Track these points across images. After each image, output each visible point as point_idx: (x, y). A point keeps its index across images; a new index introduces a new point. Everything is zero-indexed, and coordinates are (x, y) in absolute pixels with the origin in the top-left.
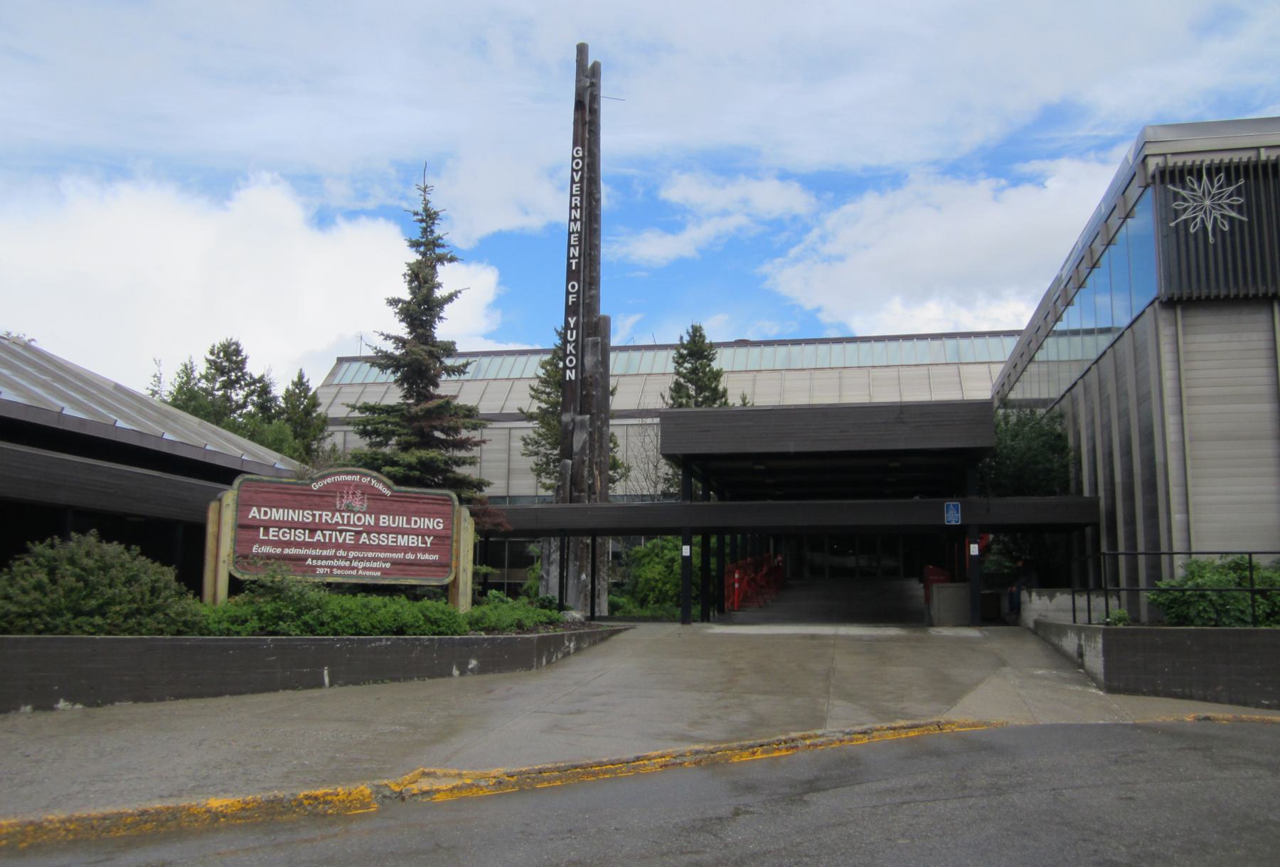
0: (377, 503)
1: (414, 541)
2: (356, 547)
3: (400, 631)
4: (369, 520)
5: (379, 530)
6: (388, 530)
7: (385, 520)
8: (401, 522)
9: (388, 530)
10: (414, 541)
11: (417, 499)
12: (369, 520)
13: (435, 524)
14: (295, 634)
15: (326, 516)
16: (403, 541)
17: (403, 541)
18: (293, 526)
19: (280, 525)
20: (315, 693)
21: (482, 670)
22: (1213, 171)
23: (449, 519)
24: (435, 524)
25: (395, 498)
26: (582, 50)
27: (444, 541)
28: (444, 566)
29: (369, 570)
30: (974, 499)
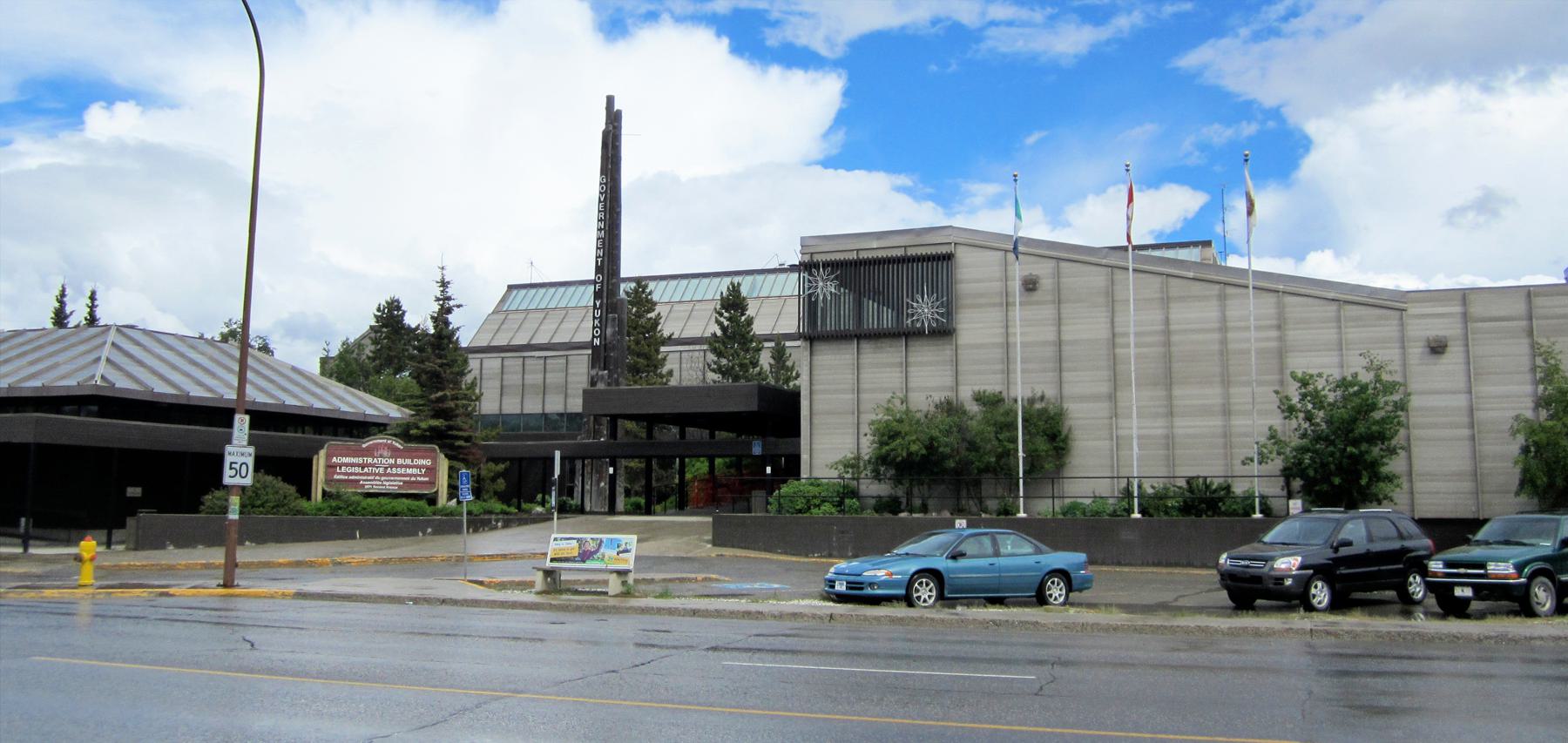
0: (396, 453)
1: (415, 471)
2: (385, 475)
3: (395, 515)
4: (392, 461)
5: (397, 466)
6: (401, 466)
7: (400, 461)
8: (408, 462)
9: (401, 466)
10: (415, 471)
11: (417, 450)
12: (392, 461)
13: (427, 462)
14: (345, 516)
15: (370, 460)
16: (409, 471)
17: (409, 471)
18: (353, 465)
19: (347, 465)
20: (351, 543)
21: (434, 533)
22: (826, 265)
23: (434, 460)
24: (427, 462)
25: (406, 450)
26: (444, 284)
27: (432, 471)
28: (432, 483)
29: (391, 486)
30: (772, 439)
